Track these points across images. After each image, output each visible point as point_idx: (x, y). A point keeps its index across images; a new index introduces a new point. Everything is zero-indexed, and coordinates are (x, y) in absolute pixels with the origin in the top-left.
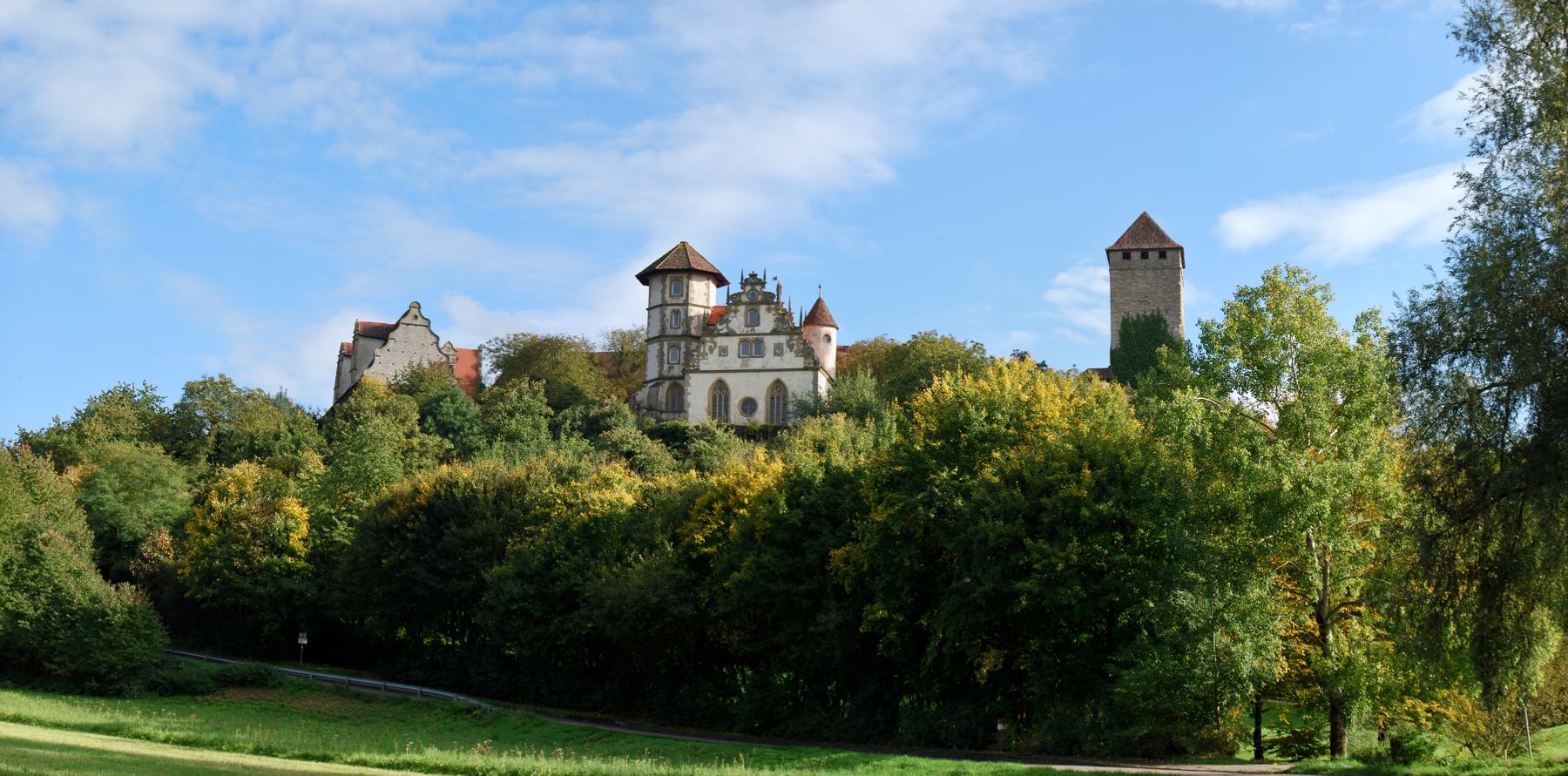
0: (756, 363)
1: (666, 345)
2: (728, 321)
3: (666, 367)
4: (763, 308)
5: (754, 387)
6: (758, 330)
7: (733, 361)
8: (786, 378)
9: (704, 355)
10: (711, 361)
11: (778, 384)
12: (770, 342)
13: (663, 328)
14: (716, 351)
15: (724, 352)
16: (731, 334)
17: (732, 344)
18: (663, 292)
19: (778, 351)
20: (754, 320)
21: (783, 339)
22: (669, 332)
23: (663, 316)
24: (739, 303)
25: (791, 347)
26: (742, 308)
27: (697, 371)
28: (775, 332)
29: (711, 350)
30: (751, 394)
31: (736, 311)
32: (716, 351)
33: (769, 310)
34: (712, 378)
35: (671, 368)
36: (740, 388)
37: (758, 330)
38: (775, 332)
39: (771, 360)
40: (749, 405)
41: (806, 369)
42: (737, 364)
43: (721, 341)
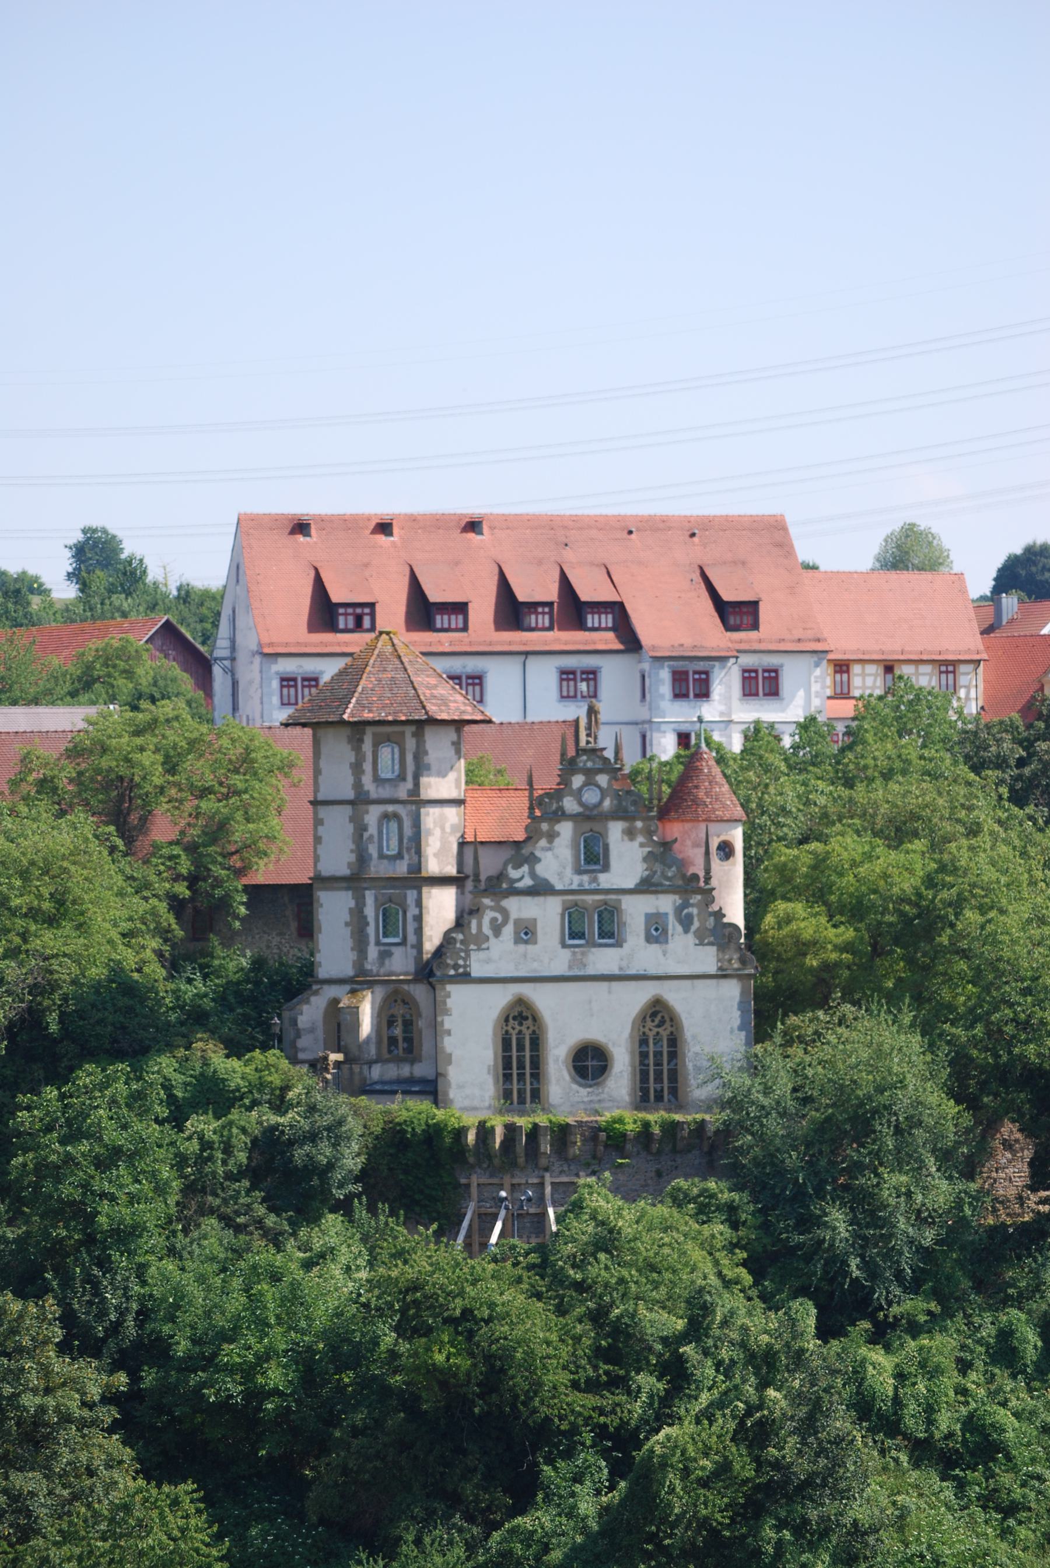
0: (604, 959)
1: (370, 897)
2: (532, 860)
3: (373, 952)
4: (615, 830)
5: (605, 1017)
6: (605, 880)
7: (550, 954)
8: (675, 996)
9: (480, 940)
10: (499, 955)
11: (658, 1013)
12: (636, 910)
13: (362, 858)
14: (508, 930)
15: (526, 933)
16: (541, 889)
17: (547, 913)
18: (357, 768)
19: (656, 931)
20: (593, 856)
21: (666, 903)
22: (378, 868)
23: (360, 829)
24: (560, 815)
25: (686, 923)
26: (566, 829)
27: (465, 978)
28: (646, 887)
29: (497, 930)
30: (595, 1033)
31: (552, 836)
32: (508, 930)
33: (630, 834)
34: (500, 998)
35: (385, 955)
36: (571, 1019)
37: (605, 880)
38: (646, 887)
39: (636, 952)
40: (590, 1062)
41: (722, 975)
42: (560, 962)
43: (519, 908)
